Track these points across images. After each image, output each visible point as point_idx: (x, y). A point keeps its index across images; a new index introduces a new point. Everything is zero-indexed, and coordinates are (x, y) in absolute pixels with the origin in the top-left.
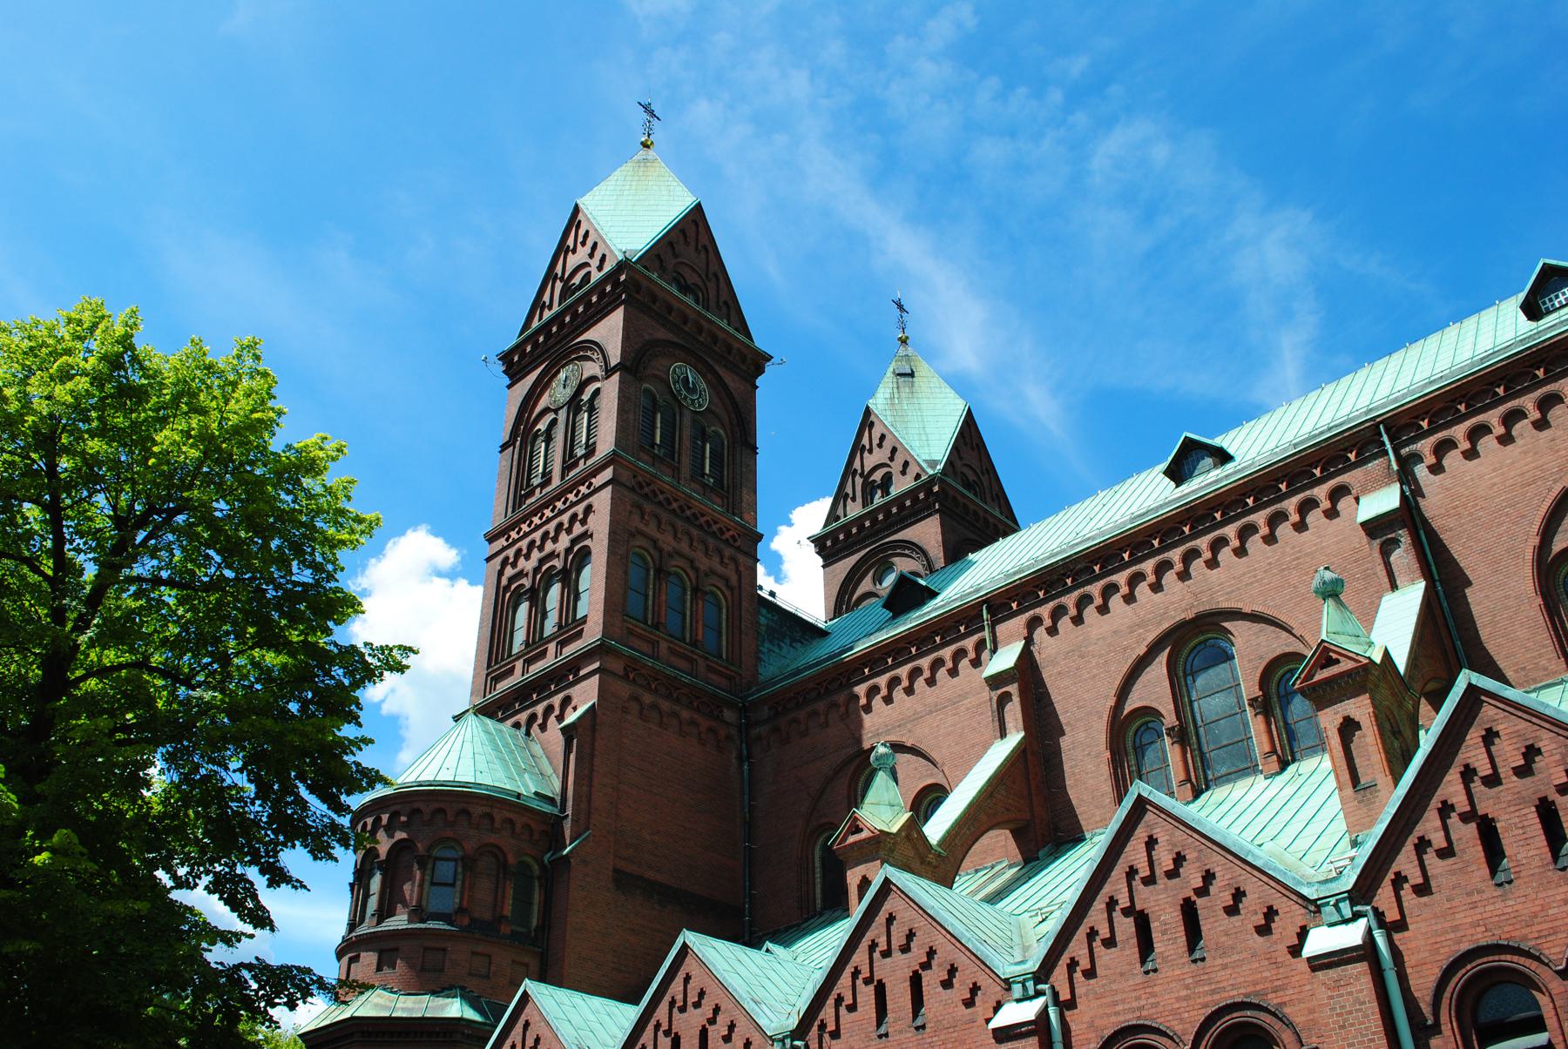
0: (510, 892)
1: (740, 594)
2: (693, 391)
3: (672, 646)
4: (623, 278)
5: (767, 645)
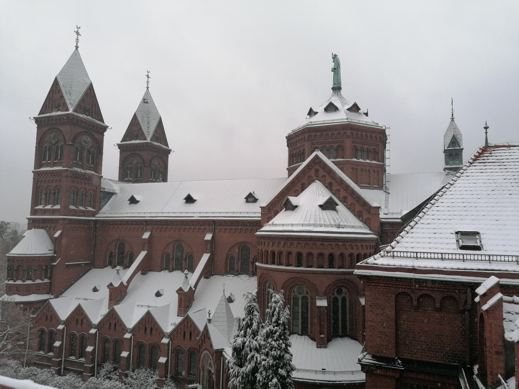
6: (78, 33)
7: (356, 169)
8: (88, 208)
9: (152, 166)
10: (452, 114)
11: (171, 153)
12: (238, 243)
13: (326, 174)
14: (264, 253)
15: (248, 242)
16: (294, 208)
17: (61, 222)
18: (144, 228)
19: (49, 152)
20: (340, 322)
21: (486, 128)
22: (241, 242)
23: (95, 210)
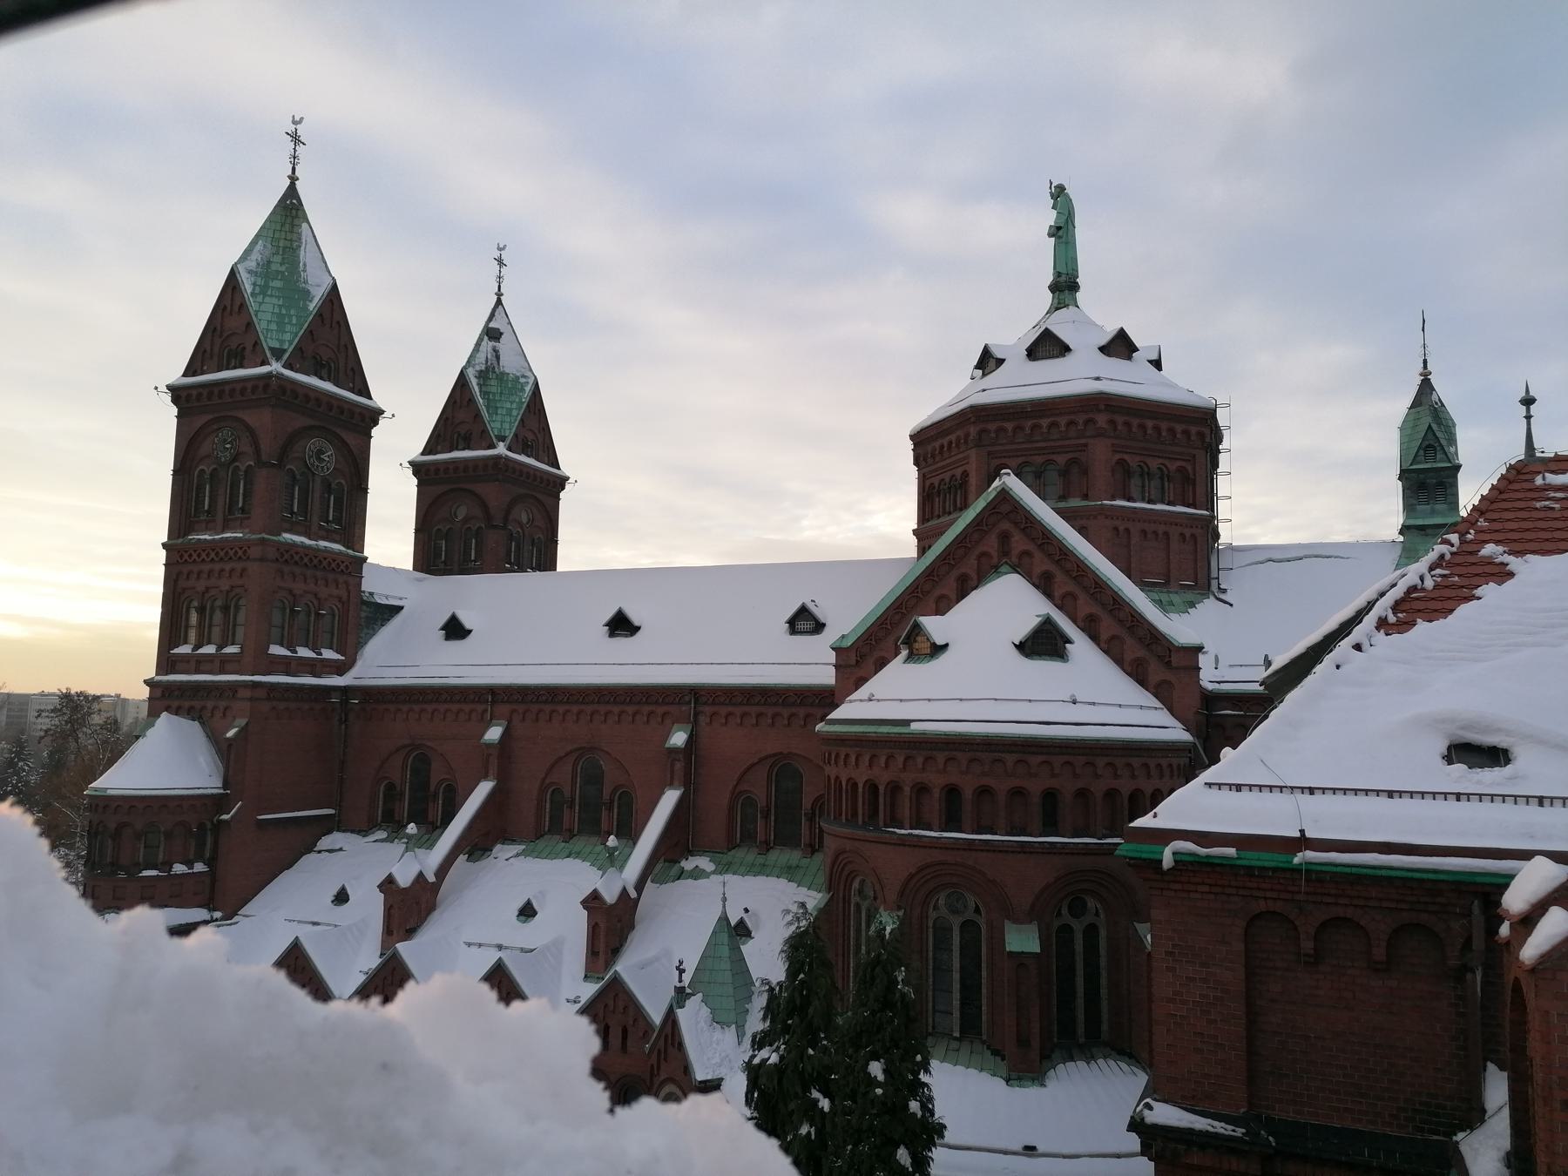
5: (365, 631)
6: (296, 138)
7: (1127, 530)
8: (323, 651)
9: (510, 527)
10: (1425, 362)
11: (568, 487)
12: (766, 757)
13: (1031, 547)
14: (844, 787)
15: (796, 754)
16: (938, 650)
17: (247, 693)
18: (487, 710)
19: (211, 487)
20: (1080, 1002)
21: (1528, 401)
22: (774, 755)
23: (343, 658)
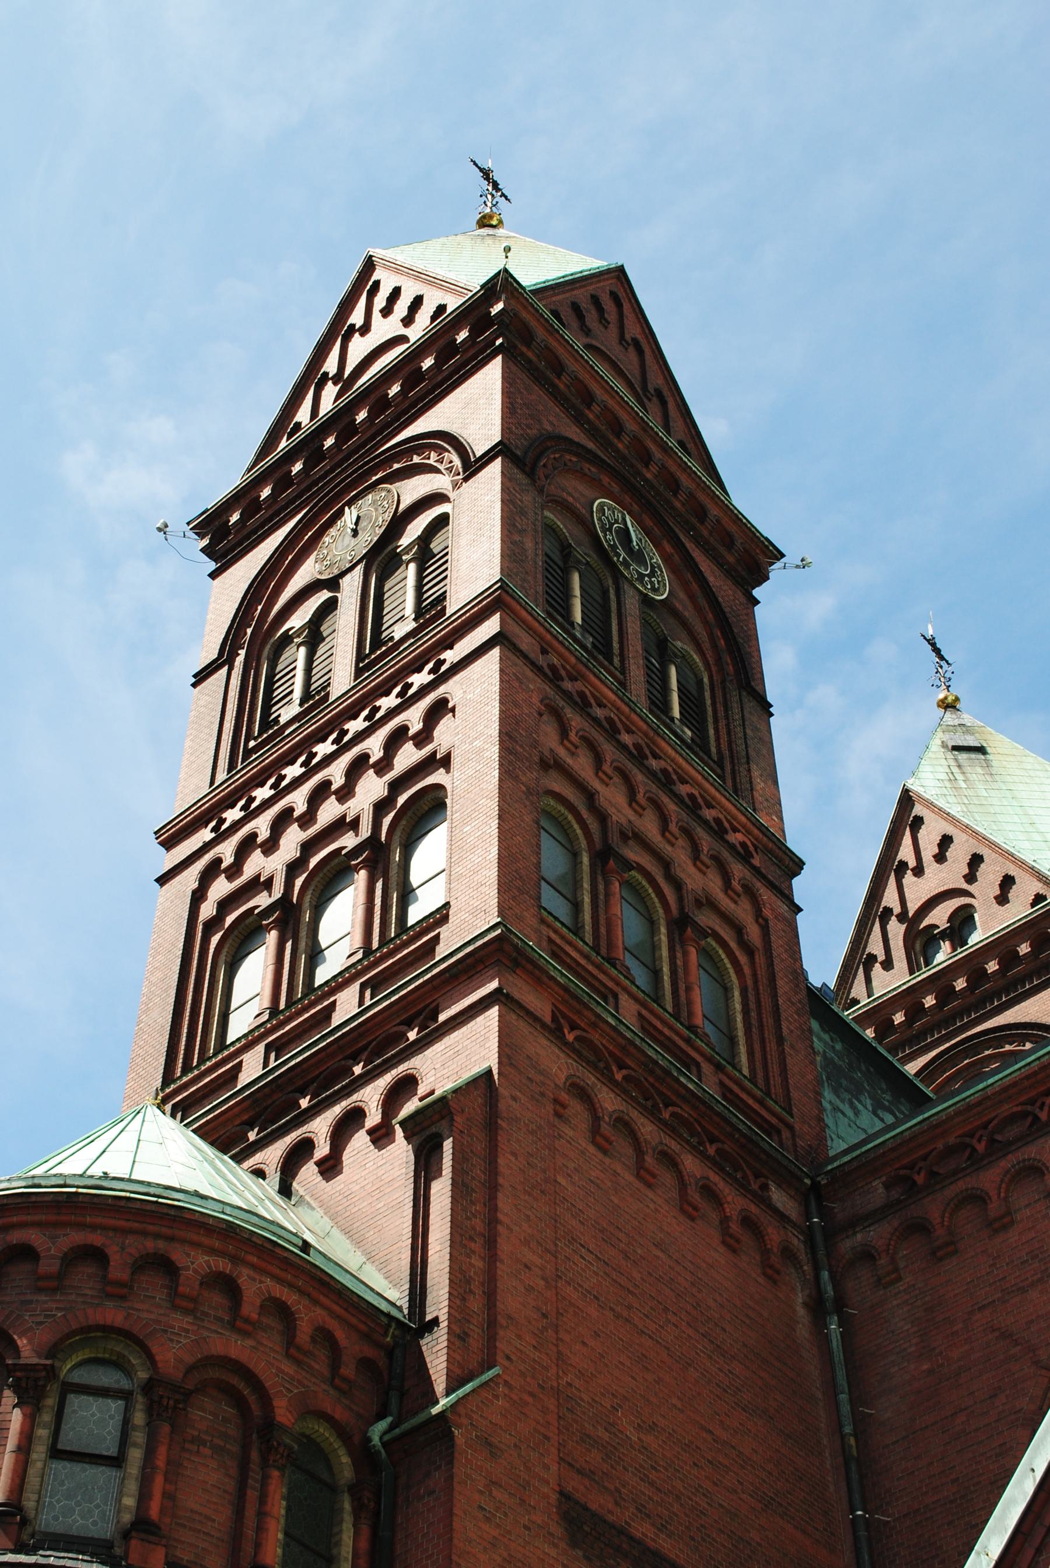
0: (278, 1507)
1: (771, 964)
2: (639, 557)
3: (644, 1012)
4: (499, 306)
